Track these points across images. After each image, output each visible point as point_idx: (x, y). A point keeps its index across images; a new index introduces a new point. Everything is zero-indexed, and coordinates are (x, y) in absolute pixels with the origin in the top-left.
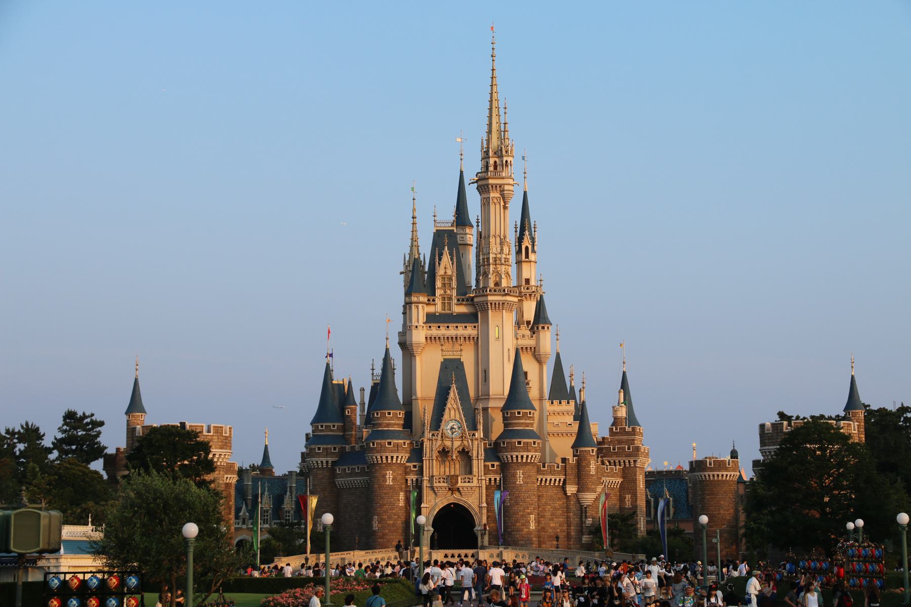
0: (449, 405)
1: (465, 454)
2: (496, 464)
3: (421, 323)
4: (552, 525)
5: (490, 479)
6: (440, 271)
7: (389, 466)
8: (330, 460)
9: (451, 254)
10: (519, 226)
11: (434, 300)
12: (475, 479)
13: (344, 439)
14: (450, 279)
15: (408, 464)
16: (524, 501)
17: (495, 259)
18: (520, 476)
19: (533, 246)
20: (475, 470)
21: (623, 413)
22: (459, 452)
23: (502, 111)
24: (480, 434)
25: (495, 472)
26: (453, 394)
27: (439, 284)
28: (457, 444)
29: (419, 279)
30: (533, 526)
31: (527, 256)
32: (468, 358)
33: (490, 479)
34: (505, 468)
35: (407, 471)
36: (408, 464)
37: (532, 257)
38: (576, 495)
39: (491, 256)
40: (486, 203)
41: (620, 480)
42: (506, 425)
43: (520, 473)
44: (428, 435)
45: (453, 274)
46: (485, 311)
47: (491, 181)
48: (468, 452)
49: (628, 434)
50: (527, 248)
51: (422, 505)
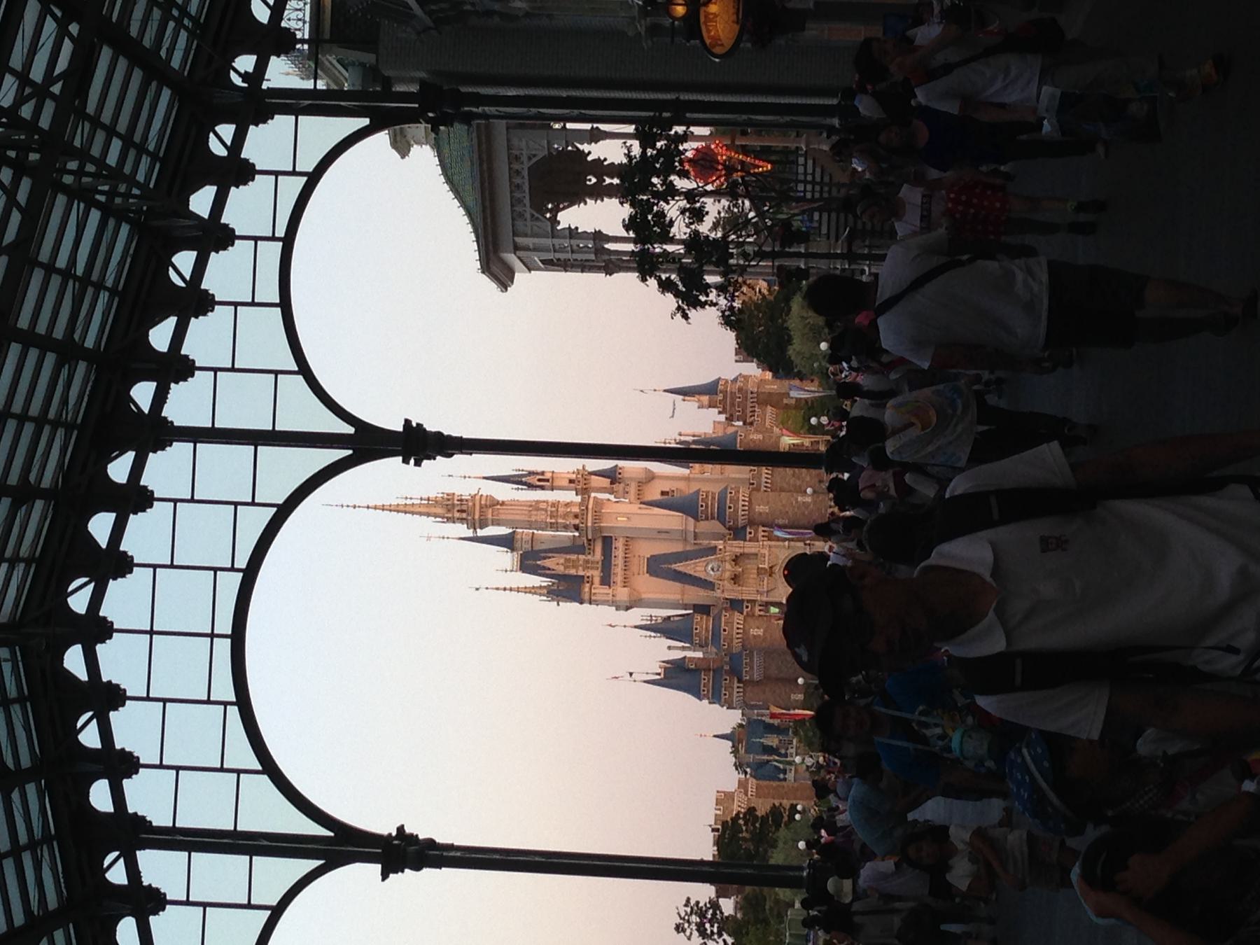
1: (736, 559)
3: (610, 591)
6: (561, 570)
7: (745, 632)
8: (736, 684)
9: (545, 558)
12: (763, 551)
13: (717, 672)
14: (567, 560)
16: (784, 506)
18: (761, 508)
19: (537, 474)
20: (753, 551)
21: (705, 399)
23: (409, 502)
24: (720, 544)
25: (756, 532)
26: (679, 567)
27: (573, 572)
28: (728, 566)
29: (567, 589)
32: (647, 549)
34: (752, 523)
35: (751, 615)
37: (548, 476)
40: (497, 523)
41: (769, 408)
42: (713, 518)
44: (718, 593)
46: (601, 529)
47: (477, 517)
49: (725, 397)
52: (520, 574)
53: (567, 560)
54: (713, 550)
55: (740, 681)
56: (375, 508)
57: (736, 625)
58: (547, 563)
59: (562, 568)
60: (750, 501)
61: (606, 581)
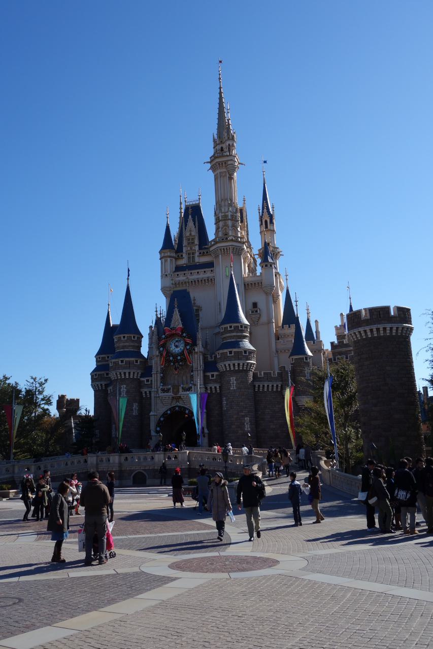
2: (215, 373)
4: (271, 426)
8: (103, 383)
10: (261, 208)
11: (182, 256)
15: (142, 379)
25: (215, 381)
27: (185, 243)
30: (247, 427)
31: (266, 227)
36: (142, 379)
43: (233, 380)
50: (266, 221)
51: (151, 413)
55: (107, 386)
56: (220, 93)
57: (127, 371)
58: (191, 223)
60: (239, 371)
61: (178, 269)
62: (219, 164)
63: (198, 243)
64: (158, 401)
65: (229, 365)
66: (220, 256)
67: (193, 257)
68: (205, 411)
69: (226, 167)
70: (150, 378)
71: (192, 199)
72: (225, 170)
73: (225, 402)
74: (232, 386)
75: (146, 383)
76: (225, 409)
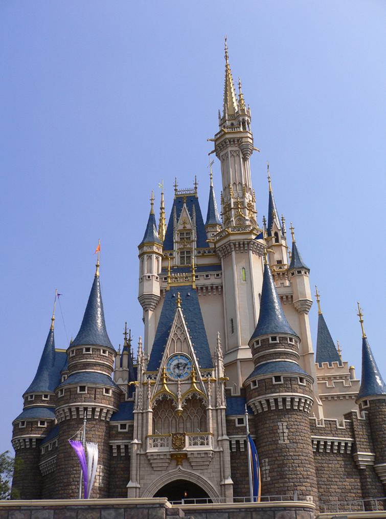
0: (172, 335)
1: (196, 403)
5: (238, 442)
6: (179, 226)
10: (267, 219)
11: (171, 254)
14: (189, 232)
15: (114, 423)
17: (236, 204)
20: (211, 425)
22: (187, 401)
27: (176, 238)
31: (277, 241)
33: (238, 442)
36: (114, 423)
38: (373, 469)
39: (232, 201)
45: (200, 243)
48: (201, 400)
50: (276, 234)
51: (130, 484)
52: (173, 197)
53: (189, 232)
54: (208, 364)
59: (181, 227)
62: (230, 142)
63: (196, 239)
64: (142, 462)
65: (276, 400)
66: (233, 253)
67: (189, 258)
68: (229, 481)
69: (239, 145)
70: (128, 423)
71: (185, 186)
72: (237, 149)
73: (268, 468)
74: (282, 438)
75: (120, 430)
76: (269, 479)
